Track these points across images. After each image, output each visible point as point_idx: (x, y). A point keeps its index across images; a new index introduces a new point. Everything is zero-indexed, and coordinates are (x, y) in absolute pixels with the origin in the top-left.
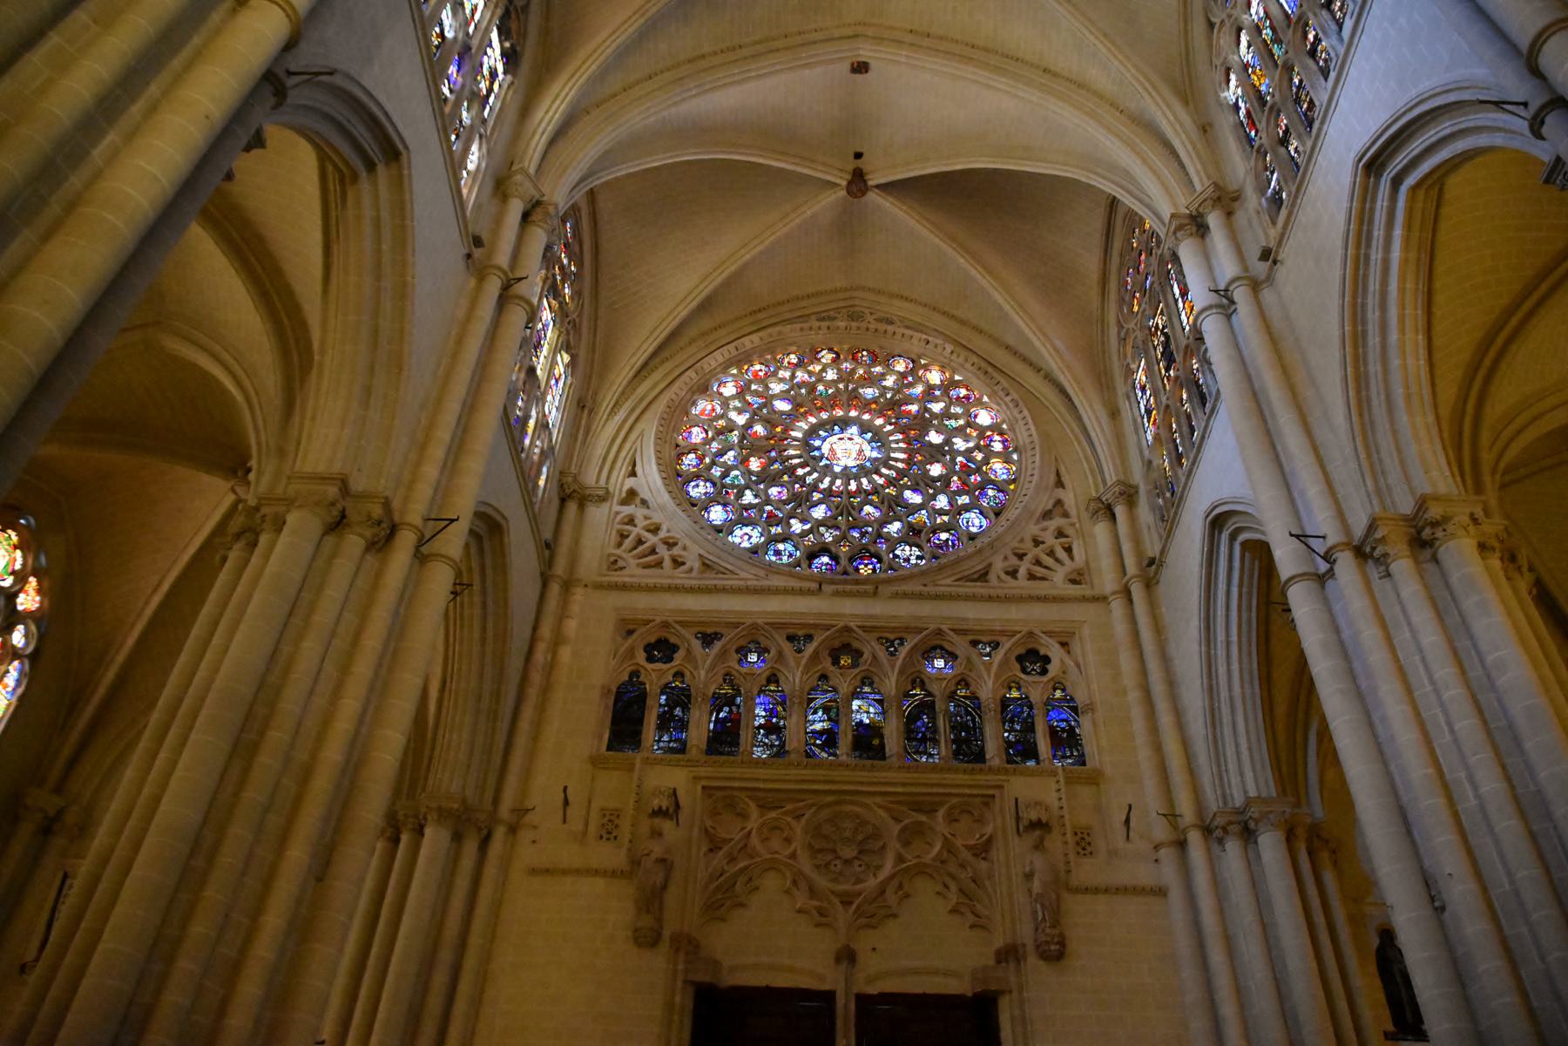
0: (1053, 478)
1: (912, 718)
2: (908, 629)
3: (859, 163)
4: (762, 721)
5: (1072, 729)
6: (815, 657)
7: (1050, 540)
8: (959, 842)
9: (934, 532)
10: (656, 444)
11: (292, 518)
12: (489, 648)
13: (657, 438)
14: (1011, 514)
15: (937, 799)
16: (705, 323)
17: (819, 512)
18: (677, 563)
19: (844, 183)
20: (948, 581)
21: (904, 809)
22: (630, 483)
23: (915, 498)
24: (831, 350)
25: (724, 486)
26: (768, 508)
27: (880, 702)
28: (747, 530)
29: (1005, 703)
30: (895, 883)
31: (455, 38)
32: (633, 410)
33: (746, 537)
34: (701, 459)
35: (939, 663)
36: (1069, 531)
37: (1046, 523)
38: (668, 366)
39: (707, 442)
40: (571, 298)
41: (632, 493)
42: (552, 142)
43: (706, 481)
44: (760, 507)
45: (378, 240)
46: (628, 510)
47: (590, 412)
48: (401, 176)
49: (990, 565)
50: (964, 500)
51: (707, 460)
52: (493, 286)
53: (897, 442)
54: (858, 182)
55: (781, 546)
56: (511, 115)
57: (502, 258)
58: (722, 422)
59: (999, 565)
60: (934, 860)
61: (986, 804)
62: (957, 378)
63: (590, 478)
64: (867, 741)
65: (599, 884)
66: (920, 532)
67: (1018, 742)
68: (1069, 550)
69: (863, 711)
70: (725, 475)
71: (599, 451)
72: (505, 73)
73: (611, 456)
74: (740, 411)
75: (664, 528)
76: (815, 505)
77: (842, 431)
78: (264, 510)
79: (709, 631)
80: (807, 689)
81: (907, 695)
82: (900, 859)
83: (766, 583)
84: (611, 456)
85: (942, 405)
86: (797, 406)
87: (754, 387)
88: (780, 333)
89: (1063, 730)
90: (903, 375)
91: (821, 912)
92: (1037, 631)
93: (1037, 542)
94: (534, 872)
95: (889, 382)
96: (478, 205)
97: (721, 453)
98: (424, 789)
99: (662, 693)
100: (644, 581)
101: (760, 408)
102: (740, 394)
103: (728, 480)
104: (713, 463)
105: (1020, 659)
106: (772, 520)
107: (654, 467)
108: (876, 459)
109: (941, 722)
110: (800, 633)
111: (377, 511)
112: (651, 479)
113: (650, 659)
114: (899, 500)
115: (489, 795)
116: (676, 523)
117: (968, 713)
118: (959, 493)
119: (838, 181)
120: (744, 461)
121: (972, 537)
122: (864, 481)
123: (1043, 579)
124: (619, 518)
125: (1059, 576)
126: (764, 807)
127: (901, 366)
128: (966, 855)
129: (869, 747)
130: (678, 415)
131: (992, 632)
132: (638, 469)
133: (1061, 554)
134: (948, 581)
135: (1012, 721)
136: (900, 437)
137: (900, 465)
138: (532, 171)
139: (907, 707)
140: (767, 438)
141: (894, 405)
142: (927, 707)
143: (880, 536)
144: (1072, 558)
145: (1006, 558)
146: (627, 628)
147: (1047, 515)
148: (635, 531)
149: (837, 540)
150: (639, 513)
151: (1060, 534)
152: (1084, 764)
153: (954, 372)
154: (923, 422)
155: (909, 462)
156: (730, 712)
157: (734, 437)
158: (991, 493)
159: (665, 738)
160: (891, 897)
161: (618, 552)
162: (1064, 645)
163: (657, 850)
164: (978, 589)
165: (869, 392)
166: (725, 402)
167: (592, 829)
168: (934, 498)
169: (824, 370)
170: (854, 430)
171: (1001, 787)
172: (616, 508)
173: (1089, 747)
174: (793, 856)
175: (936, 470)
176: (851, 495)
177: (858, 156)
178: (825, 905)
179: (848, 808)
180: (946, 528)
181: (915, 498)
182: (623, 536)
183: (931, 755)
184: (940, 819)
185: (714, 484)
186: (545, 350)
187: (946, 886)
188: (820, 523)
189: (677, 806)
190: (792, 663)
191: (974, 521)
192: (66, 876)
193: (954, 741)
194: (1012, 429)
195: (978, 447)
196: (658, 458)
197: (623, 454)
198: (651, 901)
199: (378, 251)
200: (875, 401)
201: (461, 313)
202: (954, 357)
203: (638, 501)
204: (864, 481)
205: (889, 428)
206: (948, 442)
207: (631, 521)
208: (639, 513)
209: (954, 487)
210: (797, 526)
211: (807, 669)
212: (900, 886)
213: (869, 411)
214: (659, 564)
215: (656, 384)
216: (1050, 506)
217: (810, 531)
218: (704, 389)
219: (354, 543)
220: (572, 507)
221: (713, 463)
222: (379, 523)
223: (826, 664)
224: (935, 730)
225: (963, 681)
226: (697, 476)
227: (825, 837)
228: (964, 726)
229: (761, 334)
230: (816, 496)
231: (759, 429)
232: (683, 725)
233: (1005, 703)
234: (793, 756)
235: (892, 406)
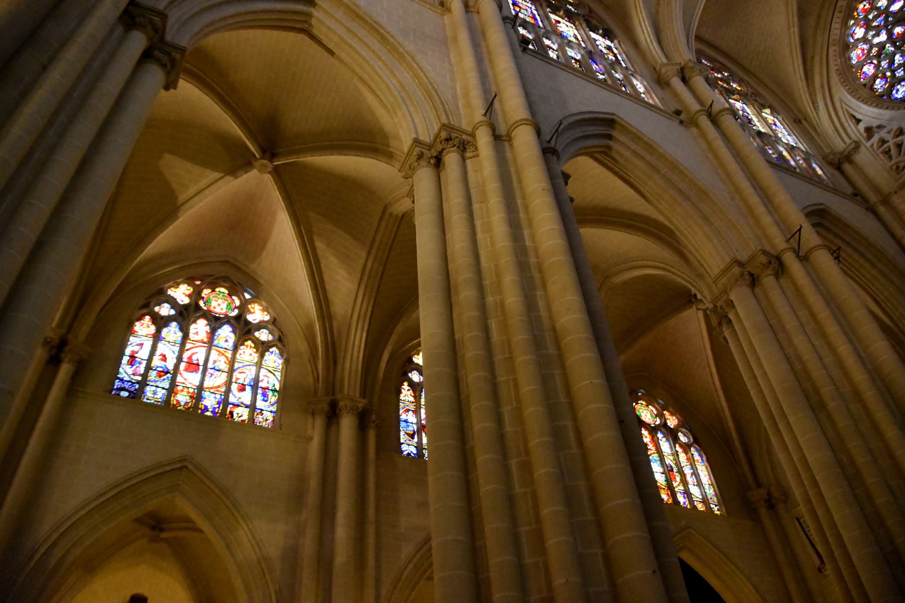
10: (853, 97)
11: (733, 297)
22: (861, 127)
31: (582, 56)
34: (884, 77)
39: (877, 67)
40: (740, 86)
41: (869, 131)
42: (659, 42)
43: (899, 84)
45: (642, 158)
46: (875, 139)
47: (806, 120)
48: (623, 126)
51: (888, 74)
52: (704, 121)
56: (633, 53)
57: (695, 106)
58: (875, 50)
63: (840, 145)
72: (612, 42)
74: (878, 34)
78: (719, 304)
87: (871, 17)
96: (662, 100)
97: (892, 62)
102: (868, 27)
104: (893, 72)
107: (865, 107)
111: (763, 259)
112: (869, 113)
130: (848, 72)
132: (859, 116)
138: (665, 61)
150: (883, 134)
157: (889, 48)
161: (893, 162)
166: (864, 40)
172: (868, 144)
182: (887, 152)
186: (755, 120)
192: (798, 520)
196: (862, 101)
197: (843, 119)
203: (876, 130)
207: (883, 141)
208: (883, 134)
218: (847, 48)
219: (769, 281)
220: (847, 167)
221: (893, 72)
222: (770, 263)
226: (892, 87)
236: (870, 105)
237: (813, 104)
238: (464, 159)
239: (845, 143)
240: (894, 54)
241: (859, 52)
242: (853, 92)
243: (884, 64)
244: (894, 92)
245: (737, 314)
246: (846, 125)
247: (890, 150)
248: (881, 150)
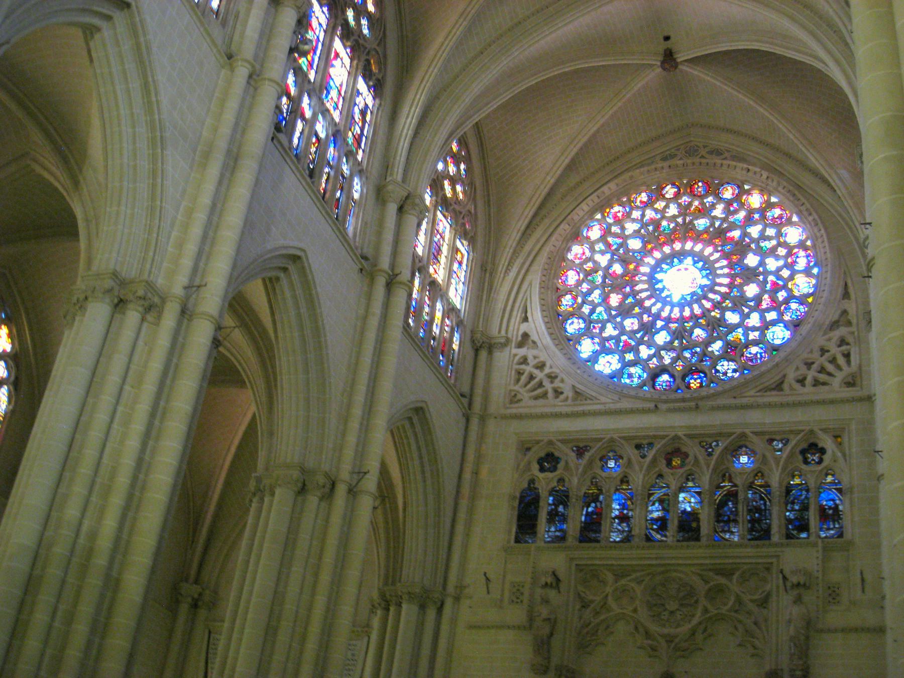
0: (840, 291)
1: (722, 504)
2: (720, 434)
3: (668, 44)
4: (617, 513)
5: (837, 506)
6: (654, 461)
7: (834, 350)
8: (746, 598)
9: (747, 347)
10: (540, 293)
11: (278, 491)
12: (429, 482)
13: (541, 287)
14: (804, 329)
15: (735, 566)
16: (573, 180)
17: (662, 338)
18: (558, 393)
19: (659, 63)
20: (752, 393)
21: (711, 574)
22: (524, 327)
23: (732, 318)
24: (673, 184)
25: (591, 322)
26: (624, 338)
27: (699, 493)
28: (609, 358)
29: (788, 489)
30: (702, 627)
31: (327, 135)
32: (524, 263)
33: (608, 365)
35: (744, 459)
36: (850, 339)
37: (831, 334)
38: (547, 221)
39: (579, 283)
41: (526, 336)
42: (416, 133)
44: (617, 339)
45: (298, 308)
46: (522, 352)
47: (491, 274)
49: (784, 376)
50: (772, 316)
51: (579, 300)
52: (381, 282)
53: (721, 268)
54: (669, 58)
55: (632, 370)
57: (385, 263)
59: (792, 375)
60: (729, 610)
61: (768, 569)
62: (774, 200)
63: (494, 331)
64: (688, 526)
66: (736, 347)
67: (796, 518)
68: (847, 356)
69: (687, 502)
70: (592, 311)
71: (500, 305)
73: (509, 308)
74: (603, 253)
75: (548, 365)
76: (658, 332)
77: (681, 261)
79: (581, 445)
80: (648, 486)
81: (719, 487)
82: (706, 611)
83: (618, 406)
84: (509, 308)
85: (759, 227)
86: (645, 244)
88: (631, 177)
89: (830, 508)
90: (729, 203)
91: (654, 649)
92: (816, 429)
93: (823, 351)
95: (718, 212)
97: (589, 292)
98: (400, 581)
99: (550, 495)
100: (533, 411)
101: (617, 250)
102: (603, 239)
103: (594, 317)
104: (584, 302)
105: (803, 452)
106: (627, 348)
107: (539, 314)
108: (705, 286)
109: (740, 507)
110: (645, 442)
112: (537, 325)
113: (542, 469)
114: (721, 321)
115: (440, 580)
116: (556, 361)
117: (762, 498)
118: (768, 310)
119: (654, 63)
120: (605, 299)
121: (776, 348)
122: (696, 306)
123: (824, 384)
124: (517, 358)
125: (836, 382)
126: (618, 576)
127: (728, 193)
128: (751, 607)
129: (690, 529)
130: (558, 263)
131: (784, 432)
132: (529, 315)
133: (841, 361)
134: (752, 393)
135: (793, 503)
136: (725, 263)
137: (724, 290)
138: (399, 178)
139: (718, 497)
140: (623, 276)
141: (721, 233)
142: (732, 495)
143: (705, 355)
144: (849, 362)
145: (797, 368)
146: (525, 448)
147: (834, 325)
148: (528, 369)
149: (674, 360)
151: (842, 342)
152: (841, 535)
153: (770, 195)
154: (742, 248)
155: (731, 286)
156: (596, 506)
157: (598, 278)
158: (794, 306)
159: (553, 529)
160: (699, 637)
161: (516, 388)
162: (836, 437)
163: (544, 612)
164: (773, 398)
165: (701, 223)
167: (506, 600)
168: (748, 316)
169: (667, 206)
170: (689, 260)
171: (778, 556)
172: (514, 351)
173: (846, 521)
174: (635, 611)
175: (751, 290)
176: (687, 320)
177: (667, 38)
178: (655, 643)
179: (674, 574)
180: (756, 343)
181: (732, 318)
182: (520, 373)
183: (732, 533)
184: (735, 581)
185: (585, 321)
187: (736, 628)
188: (659, 348)
189: (558, 580)
190: (637, 468)
191: (779, 335)
192: (210, 632)
193: (749, 521)
194: (814, 246)
195: (786, 266)
197: (517, 305)
198: (543, 646)
199: (299, 315)
200: (706, 231)
201: (361, 312)
202: (770, 182)
204: (696, 306)
205: (717, 255)
206: (762, 263)
207: (524, 361)
209: (764, 305)
210: (644, 352)
211: (649, 470)
212: (705, 630)
213: (702, 241)
214: (545, 395)
215: (538, 241)
216: (836, 317)
217: (654, 355)
218: (576, 236)
219: (313, 500)
220: (483, 354)
221: (584, 302)
222: (324, 487)
223: (662, 465)
224: (736, 513)
225: (759, 473)
226: (572, 315)
227: (658, 595)
228: (758, 509)
229: (616, 181)
230: (660, 324)
231: (618, 268)
232: (564, 519)
233: (788, 489)
234: (636, 540)
235: (718, 235)
236: (544, 317)
237: (509, 265)
238: (143, 319)
239: (500, 332)
240: (596, 288)
241: (581, 252)
242: (544, 287)
243: (585, 287)
244: (569, 321)
245: (271, 502)
246: (515, 313)
247: (523, 374)
248: (517, 367)
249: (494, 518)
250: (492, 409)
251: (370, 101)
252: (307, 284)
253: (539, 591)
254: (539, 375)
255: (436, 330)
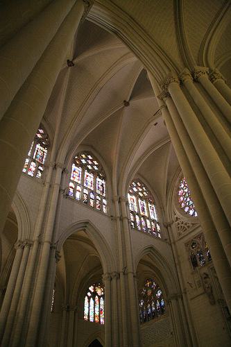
18: (189, 227)
22: (176, 216)
41: (177, 218)
56: (110, 186)
65: (202, 297)
94: (192, 299)
116: (185, 219)
130: (178, 197)
138: (116, 194)
146: (186, 245)
189: (207, 275)
198: (211, 295)
218: (179, 189)
219: (114, 281)
220: (169, 228)
249: (186, 266)
250: (176, 239)
251: (104, 182)
252: (93, 227)
253: (204, 280)
254: (183, 225)
255: (149, 227)
